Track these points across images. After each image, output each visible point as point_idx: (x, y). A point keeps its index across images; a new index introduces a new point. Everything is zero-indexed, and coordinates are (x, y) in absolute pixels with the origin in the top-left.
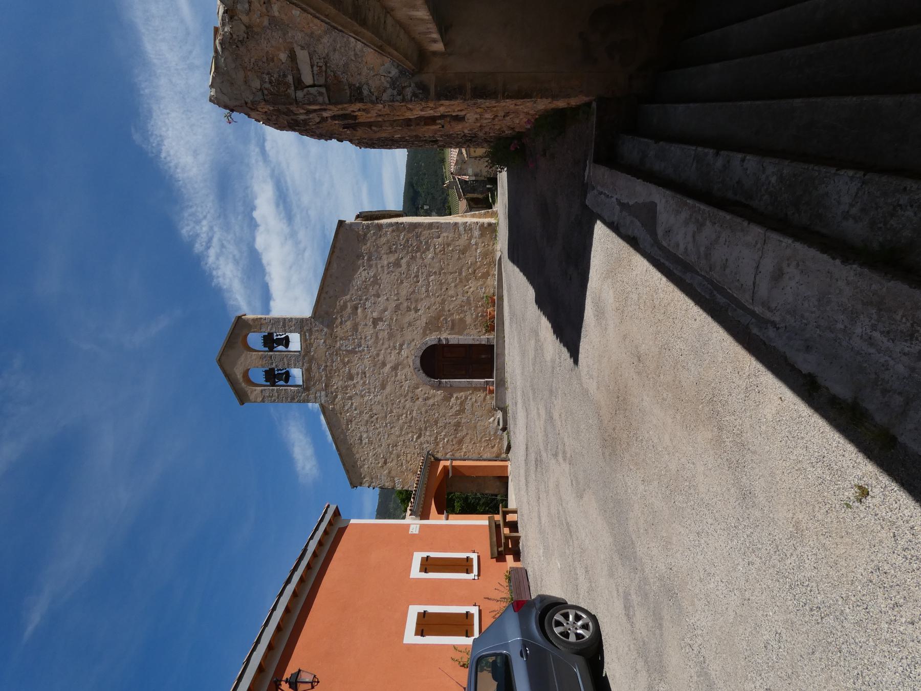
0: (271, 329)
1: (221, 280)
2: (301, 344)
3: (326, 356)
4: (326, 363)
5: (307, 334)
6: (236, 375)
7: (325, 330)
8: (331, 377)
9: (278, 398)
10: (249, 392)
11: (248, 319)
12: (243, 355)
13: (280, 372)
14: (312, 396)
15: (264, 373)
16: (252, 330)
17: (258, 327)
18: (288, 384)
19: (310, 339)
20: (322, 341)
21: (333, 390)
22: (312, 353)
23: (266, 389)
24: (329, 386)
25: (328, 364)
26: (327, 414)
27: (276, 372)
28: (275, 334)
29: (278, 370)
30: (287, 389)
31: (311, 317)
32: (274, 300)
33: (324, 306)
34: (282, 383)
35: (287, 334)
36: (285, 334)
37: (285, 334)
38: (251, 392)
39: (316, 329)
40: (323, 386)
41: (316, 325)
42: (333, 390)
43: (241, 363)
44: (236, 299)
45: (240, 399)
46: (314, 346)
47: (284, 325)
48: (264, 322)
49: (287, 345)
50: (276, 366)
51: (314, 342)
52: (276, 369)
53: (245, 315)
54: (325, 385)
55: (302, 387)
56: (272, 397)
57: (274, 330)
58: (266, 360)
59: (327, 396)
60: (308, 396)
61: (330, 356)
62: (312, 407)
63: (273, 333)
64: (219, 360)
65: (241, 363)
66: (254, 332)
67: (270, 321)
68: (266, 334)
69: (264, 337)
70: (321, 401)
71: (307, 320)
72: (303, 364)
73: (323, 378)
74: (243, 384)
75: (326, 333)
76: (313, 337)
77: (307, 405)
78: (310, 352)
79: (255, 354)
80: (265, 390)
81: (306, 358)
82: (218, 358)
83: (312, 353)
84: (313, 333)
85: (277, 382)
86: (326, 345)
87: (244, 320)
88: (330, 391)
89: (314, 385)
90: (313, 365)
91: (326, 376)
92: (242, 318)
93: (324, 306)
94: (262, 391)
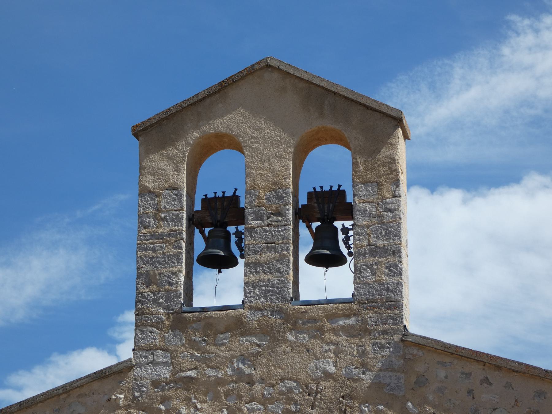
0: (364, 212)
1: (529, 39)
2: (318, 303)
3: (282, 380)
4: (262, 380)
5: (351, 321)
6: (222, 116)
7: (367, 378)
8: (216, 398)
9: (153, 235)
10: (171, 151)
11: (393, 146)
12: (284, 135)
13: (233, 239)
14: (156, 337)
15: (229, 193)
16: (360, 160)
17: (371, 176)
18: (196, 265)
19: (334, 331)
20: (331, 369)
21: (175, 403)
22: (290, 337)
23: (180, 202)
24: (188, 390)
25: (258, 388)
26: (96, 385)
27: (232, 229)
28: (348, 224)
29: (239, 234)
30: (179, 262)
31: (405, 332)
32: (465, 202)
33: (442, 374)
34: (200, 245)
35: (349, 259)
36: (350, 254)
37: (350, 254)
38: (170, 158)
39: (369, 349)
40: (189, 373)
41: (382, 347)
42: (175, 403)
43: (259, 129)
44: (469, 86)
45: (151, 126)
46: (316, 342)
47: (375, 251)
48: (386, 193)
49: (313, 260)
50: (252, 229)
51: (328, 344)
52: (241, 228)
53: (406, 137)
54: (190, 378)
55: (185, 308)
56: (155, 217)
57: (362, 221)
58: (268, 199)
59: (156, 384)
60: (158, 325)
61: (282, 393)
62: (125, 324)
63: (352, 218)
64: (269, 66)
65: (259, 129)
66: (355, 164)
67: (390, 210)
68: (349, 199)
69: (341, 193)
70: (139, 365)
71: (398, 319)
72: (260, 310)
73: (212, 373)
74: (197, 135)
75: (354, 381)
76: (342, 339)
77: (129, 309)
78: (295, 329)
79: (286, 167)
80: (179, 196)
81: (275, 320)
82: (274, 63)
83: (290, 337)
84: (356, 340)
85: (202, 232)
86: (317, 381)
87: (390, 135)
88: (172, 393)
89: (193, 344)
90: (256, 340)
91: (220, 382)
92: (395, 129)
93: (442, 374)
94: (174, 188)
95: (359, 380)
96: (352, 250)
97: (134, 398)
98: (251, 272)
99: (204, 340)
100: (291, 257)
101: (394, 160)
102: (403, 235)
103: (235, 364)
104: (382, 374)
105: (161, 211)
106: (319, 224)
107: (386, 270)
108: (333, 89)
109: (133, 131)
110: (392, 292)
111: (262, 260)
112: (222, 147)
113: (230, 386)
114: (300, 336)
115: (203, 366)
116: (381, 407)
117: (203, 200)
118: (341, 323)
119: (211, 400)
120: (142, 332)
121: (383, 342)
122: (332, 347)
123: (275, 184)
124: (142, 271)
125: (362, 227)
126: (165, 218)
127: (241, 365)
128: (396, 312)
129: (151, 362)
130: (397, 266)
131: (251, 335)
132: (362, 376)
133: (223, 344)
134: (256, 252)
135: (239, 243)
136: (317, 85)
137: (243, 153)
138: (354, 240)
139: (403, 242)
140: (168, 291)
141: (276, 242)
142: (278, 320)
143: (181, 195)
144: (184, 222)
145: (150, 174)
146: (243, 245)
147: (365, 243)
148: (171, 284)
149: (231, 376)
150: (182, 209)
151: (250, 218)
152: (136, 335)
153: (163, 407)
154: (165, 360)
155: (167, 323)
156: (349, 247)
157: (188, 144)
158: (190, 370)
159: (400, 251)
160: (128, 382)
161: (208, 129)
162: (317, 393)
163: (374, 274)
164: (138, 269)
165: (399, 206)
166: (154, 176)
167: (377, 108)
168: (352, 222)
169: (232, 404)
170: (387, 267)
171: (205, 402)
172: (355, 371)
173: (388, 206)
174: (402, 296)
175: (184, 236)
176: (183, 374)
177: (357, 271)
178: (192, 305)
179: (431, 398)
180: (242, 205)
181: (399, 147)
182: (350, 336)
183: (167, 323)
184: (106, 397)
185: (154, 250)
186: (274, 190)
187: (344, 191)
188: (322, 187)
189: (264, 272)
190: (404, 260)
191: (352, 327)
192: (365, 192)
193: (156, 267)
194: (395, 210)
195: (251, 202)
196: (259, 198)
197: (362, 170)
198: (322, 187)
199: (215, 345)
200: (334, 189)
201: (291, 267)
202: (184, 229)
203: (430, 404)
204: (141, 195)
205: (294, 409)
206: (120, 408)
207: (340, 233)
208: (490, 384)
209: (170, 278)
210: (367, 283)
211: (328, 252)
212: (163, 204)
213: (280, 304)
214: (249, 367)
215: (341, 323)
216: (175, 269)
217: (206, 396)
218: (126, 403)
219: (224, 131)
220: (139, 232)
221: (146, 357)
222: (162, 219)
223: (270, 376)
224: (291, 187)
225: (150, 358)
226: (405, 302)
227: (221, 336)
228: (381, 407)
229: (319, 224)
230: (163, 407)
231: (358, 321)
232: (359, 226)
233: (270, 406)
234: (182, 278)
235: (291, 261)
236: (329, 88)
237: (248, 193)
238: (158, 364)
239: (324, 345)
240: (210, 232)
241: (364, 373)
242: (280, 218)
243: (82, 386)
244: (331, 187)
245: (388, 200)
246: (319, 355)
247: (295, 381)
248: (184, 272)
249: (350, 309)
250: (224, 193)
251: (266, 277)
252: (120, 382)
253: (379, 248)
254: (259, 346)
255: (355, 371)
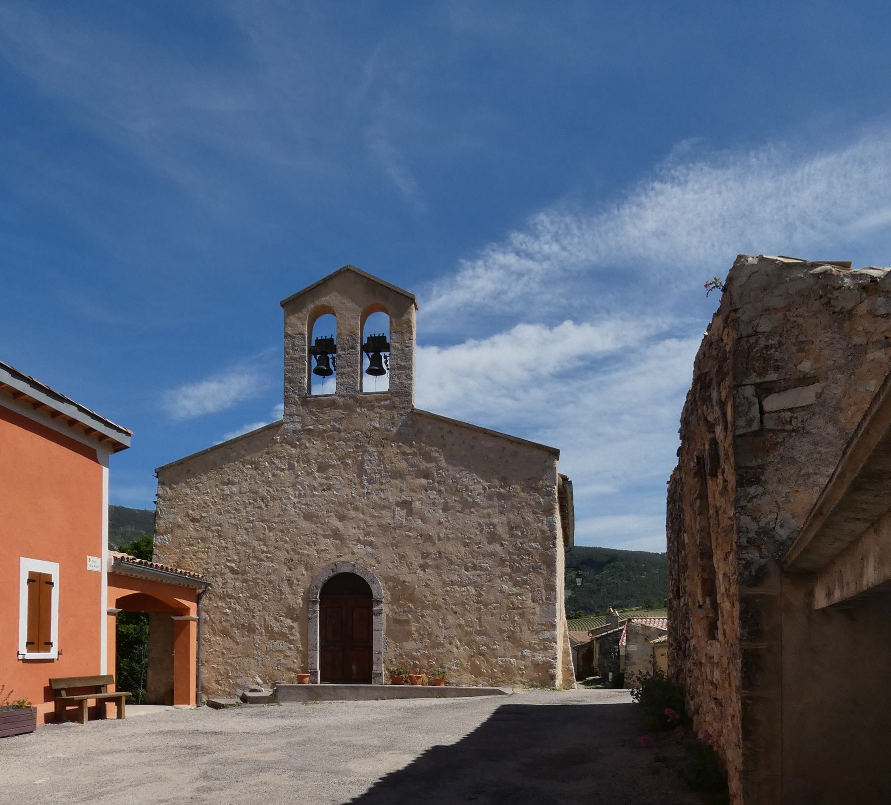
0: (395, 348)
1: (469, 273)
2: (372, 393)
3: (354, 431)
4: (345, 431)
5: (387, 402)
6: (325, 296)
7: (394, 430)
8: (323, 439)
9: (292, 358)
10: (300, 315)
11: (410, 314)
12: (356, 306)
13: (331, 361)
14: (294, 409)
15: (328, 337)
16: (394, 320)
17: (399, 329)
18: (312, 373)
19: (380, 407)
20: (378, 425)
21: (303, 441)
22: (358, 410)
23: (304, 341)
24: (309, 435)
25: (343, 434)
26: (266, 432)
27: (330, 356)
28: (387, 354)
29: (333, 358)
30: (305, 372)
31: (413, 409)
32: (439, 352)
33: (430, 428)
34: (314, 364)
35: (387, 371)
36: (388, 369)
37: (388, 369)
38: (299, 318)
39: (396, 416)
40: (310, 427)
41: (402, 415)
42: (303, 441)
43: (343, 303)
44: (440, 296)
45: (290, 301)
46: (370, 413)
47: (401, 368)
48: (406, 338)
49: (371, 372)
50: (340, 356)
51: (376, 413)
52: (335, 355)
53: (416, 309)
54: (311, 429)
55: (308, 395)
56: (293, 349)
57: (393, 352)
58: (348, 340)
59: (294, 432)
60: (295, 403)
61: (354, 437)
63: (389, 351)
64: (349, 270)
65: (343, 303)
66: (391, 322)
67: (408, 347)
68: (388, 341)
69: (384, 338)
70: (286, 423)
71: (410, 402)
72: (343, 396)
73: (321, 427)
74: (313, 306)
75: (388, 431)
76: (383, 411)
78: (361, 406)
79: (357, 323)
80: (304, 338)
81: (351, 401)
82: (351, 268)
83: (358, 410)
84: (390, 411)
85: (316, 357)
86: (371, 431)
87: (408, 307)
88: (302, 436)
89: (312, 413)
90: (342, 411)
91: (325, 431)
92: (411, 305)
93: (430, 428)
94: (302, 334)
95: (391, 431)
96: (389, 367)
97: (285, 438)
98: (339, 378)
99: (317, 411)
100: (359, 370)
101: (410, 320)
102: (413, 360)
103: (332, 423)
104: (402, 428)
105: (295, 346)
106: (373, 353)
107: (405, 377)
108: (380, 283)
109: (281, 304)
110: (407, 388)
111: (345, 372)
112: (325, 313)
113: (330, 433)
114: (363, 409)
115: (317, 423)
116: (401, 444)
117: (315, 340)
118: (382, 403)
119: (321, 440)
120: (287, 407)
121: (402, 413)
122: (378, 415)
123: (351, 332)
124: (287, 376)
125: (394, 355)
126: (297, 350)
127: (335, 424)
128: (409, 398)
129: (292, 421)
130: (410, 375)
131: (339, 409)
132: (392, 429)
133: (326, 413)
134: (342, 368)
135: (333, 363)
136: (372, 280)
137: (335, 316)
138: (390, 361)
139: (413, 363)
140: (300, 387)
141: (352, 362)
142: (352, 402)
143: (305, 337)
144: (307, 352)
145: (289, 326)
146: (335, 364)
147: (395, 363)
148: (301, 383)
149: (330, 429)
150: (305, 345)
151: (339, 350)
152: (284, 408)
153: (298, 443)
154: (298, 421)
155: (299, 402)
156: (387, 366)
157: (308, 311)
158: (310, 425)
159: (411, 368)
160: (281, 431)
161: (318, 303)
162: (370, 437)
163: (399, 379)
164: (285, 375)
165: (412, 345)
166: (292, 327)
167: (402, 293)
168: (389, 353)
169: (330, 442)
170: (406, 376)
171: (318, 441)
172: (389, 427)
173: (407, 345)
174: (412, 390)
175: (307, 359)
176: (307, 427)
177: (391, 377)
178: (311, 394)
179: (424, 439)
180: (335, 344)
181: (413, 314)
182: (386, 410)
183: (299, 402)
184: (271, 438)
185: (292, 366)
186: (351, 336)
187: (385, 337)
188: (374, 334)
189: (346, 378)
190: (413, 373)
191: (388, 405)
192: (396, 337)
193: (293, 374)
194: (410, 346)
195: (339, 342)
196: (343, 339)
197: (394, 325)
198: (374, 334)
199: (323, 413)
200: (380, 335)
201: (359, 375)
202: (307, 355)
203: (423, 443)
204: (285, 337)
205: (359, 445)
206: (278, 443)
207: (383, 358)
208: (452, 433)
209: (300, 380)
210: (395, 384)
211: (377, 368)
212: (296, 342)
213: (353, 394)
214: (339, 424)
215: (382, 403)
216: (302, 376)
217: (318, 438)
218: (280, 441)
219: (326, 304)
220: (285, 356)
221: (290, 419)
222: (296, 350)
223: (348, 428)
224: (359, 334)
225: (291, 419)
226: (413, 393)
227: (325, 409)
228: (401, 444)
229: (373, 353)
230: (298, 443)
231: (390, 402)
232: (393, 355)
233: (348, 443)
234: (306, 380)
235: (359, 373)
236: (378, 282)
237: (338, 336)
238: (296, 422)
239: (374, 414)
240: (319, 357)
241: (393, 428)
242: (354, 350)
243: (259, 432)
244: (379, 334)
245: (407, 342)
246: (372, 419)
247: (361, 431)
248: (307, 377)
249: (387, 396)
250: (326, 337)
251: (347, 380)
252: (278, 431)
253: (402, 366)
254: (343, 414)
255: (389, 427)
